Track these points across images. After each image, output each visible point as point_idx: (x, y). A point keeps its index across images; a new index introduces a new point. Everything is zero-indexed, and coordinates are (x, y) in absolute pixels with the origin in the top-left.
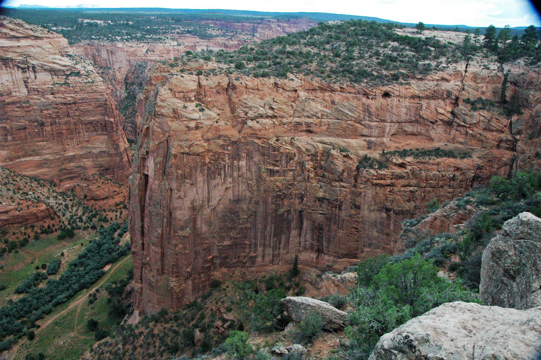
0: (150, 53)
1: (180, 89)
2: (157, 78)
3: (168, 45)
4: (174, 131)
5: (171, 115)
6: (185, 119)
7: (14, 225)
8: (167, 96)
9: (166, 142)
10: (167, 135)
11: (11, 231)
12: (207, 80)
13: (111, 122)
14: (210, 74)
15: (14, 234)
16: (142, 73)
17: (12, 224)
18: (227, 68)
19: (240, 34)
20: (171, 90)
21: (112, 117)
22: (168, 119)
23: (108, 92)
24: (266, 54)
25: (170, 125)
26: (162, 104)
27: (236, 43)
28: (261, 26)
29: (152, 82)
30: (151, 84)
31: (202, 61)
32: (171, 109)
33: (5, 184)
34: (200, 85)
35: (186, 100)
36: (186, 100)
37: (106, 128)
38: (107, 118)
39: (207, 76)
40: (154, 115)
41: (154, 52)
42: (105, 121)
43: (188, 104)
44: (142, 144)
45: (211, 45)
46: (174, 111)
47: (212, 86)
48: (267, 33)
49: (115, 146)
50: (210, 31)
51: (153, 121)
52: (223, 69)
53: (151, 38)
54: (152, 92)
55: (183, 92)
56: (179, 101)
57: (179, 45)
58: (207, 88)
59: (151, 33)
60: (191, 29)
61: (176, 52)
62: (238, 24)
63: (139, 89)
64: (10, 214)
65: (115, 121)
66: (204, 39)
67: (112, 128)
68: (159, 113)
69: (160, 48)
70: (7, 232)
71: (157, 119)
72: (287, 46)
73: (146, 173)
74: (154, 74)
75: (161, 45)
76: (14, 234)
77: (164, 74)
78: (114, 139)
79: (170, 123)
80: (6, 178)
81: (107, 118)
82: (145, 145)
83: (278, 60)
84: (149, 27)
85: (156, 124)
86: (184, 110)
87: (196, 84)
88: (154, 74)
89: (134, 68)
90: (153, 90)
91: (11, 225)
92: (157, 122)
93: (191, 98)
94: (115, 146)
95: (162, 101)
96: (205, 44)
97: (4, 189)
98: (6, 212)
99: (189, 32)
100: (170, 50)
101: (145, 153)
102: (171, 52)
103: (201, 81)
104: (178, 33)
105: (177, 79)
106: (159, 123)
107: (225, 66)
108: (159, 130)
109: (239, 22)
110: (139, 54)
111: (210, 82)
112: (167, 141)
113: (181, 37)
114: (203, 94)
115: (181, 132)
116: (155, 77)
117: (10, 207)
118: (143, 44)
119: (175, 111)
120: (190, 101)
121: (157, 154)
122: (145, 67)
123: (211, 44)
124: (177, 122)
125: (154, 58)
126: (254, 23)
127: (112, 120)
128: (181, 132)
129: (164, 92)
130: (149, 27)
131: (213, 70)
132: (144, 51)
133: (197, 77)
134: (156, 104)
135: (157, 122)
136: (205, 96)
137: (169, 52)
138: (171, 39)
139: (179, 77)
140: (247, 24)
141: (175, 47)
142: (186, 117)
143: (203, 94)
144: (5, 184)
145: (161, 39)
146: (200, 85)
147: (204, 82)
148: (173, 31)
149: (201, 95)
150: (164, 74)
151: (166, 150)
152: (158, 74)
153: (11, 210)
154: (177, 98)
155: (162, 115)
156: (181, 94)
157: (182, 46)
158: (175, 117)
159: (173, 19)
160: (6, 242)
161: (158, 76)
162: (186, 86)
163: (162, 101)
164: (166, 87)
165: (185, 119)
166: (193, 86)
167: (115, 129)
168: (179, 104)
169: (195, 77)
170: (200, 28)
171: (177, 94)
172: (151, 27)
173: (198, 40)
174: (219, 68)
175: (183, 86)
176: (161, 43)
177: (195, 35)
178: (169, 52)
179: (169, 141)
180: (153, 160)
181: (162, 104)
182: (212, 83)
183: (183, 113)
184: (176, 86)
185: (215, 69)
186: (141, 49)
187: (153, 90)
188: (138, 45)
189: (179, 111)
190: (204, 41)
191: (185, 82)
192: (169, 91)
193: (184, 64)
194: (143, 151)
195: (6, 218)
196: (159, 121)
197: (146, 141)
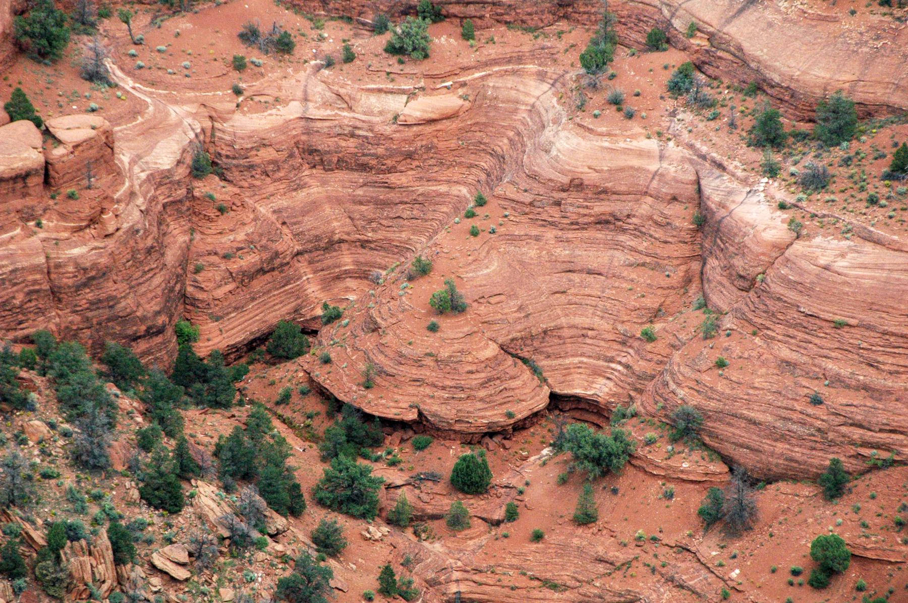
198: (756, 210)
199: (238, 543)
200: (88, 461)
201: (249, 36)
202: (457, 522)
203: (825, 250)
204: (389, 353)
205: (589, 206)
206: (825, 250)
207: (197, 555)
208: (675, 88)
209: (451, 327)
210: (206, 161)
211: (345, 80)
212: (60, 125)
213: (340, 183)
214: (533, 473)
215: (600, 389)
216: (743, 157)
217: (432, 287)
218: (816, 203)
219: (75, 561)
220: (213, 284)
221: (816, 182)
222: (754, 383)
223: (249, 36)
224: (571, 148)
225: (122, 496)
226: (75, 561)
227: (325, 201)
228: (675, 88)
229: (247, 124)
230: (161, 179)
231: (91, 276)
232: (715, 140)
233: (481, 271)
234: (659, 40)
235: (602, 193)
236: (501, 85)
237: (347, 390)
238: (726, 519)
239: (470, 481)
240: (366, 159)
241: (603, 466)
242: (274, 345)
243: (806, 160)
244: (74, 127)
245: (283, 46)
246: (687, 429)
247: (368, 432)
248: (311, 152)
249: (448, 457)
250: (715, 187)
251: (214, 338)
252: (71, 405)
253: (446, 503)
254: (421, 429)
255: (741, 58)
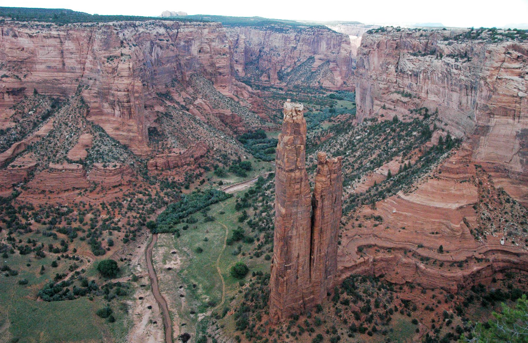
7: (521, 272)
11: (517, 278)
15: (520, 281)
17: (520, 270)
33: (522, 224)
64: (522, 257)
70: (513, 277)
76: (520, 281)
80: (523, 216)
91: (518, 271)
97: (520, 228)
98: (518, 255)
117: (523, 251)
144: (522, 224)
153: (523, 254)
160: (510, 287)
195: (516, 261)
198: (422, 266)
199: (386, 294)
200: (373, 286)
201: (376, 250)
202: (400, 292)
203: (429, 270)
204: (391, 277)
205: (406, 265)
206: (429, 270)
207: (383, 295)
208: (413, 255)
209: (398, 275)
210: (374, 261)
211: (384, 254)
212: (365, 258)
213: (384, 263)
214: (406, 288)
215: (410, 281)
216: (420, 262)
217: (395, 272)
218: (427, 266)
219: (374, 295)
220: (376, 271)
221: (427, 264)
222: (424, 281)
223: (376, 250)
224: (404, 260)
225: (376, 289)
226: (374, 295)
227: (383, 264)
228: (413, 255)
229: (377, 257)
230: (371, 262)
231: (368, 270)
232: (417, 260)
233: (399, 271)
234: (410, 251)
235: (408, 264)
236: (397, 255)
237: (389, 281)
238: (424, 292)
239: (401, 289)
240: (387, 261)
241: (412, 288)
242: (381, 276)
243: (425, 262)
244: (366, 258)
245: (379, 251)
246: (419, 285)
247: (391, 284)
248: (382, 260)
249: (398, 286)
250: (418, 264)
251: (377, 276)
252: (371, 282)
253: (399, 290)
254: (396, 284)
255: (418, 253)
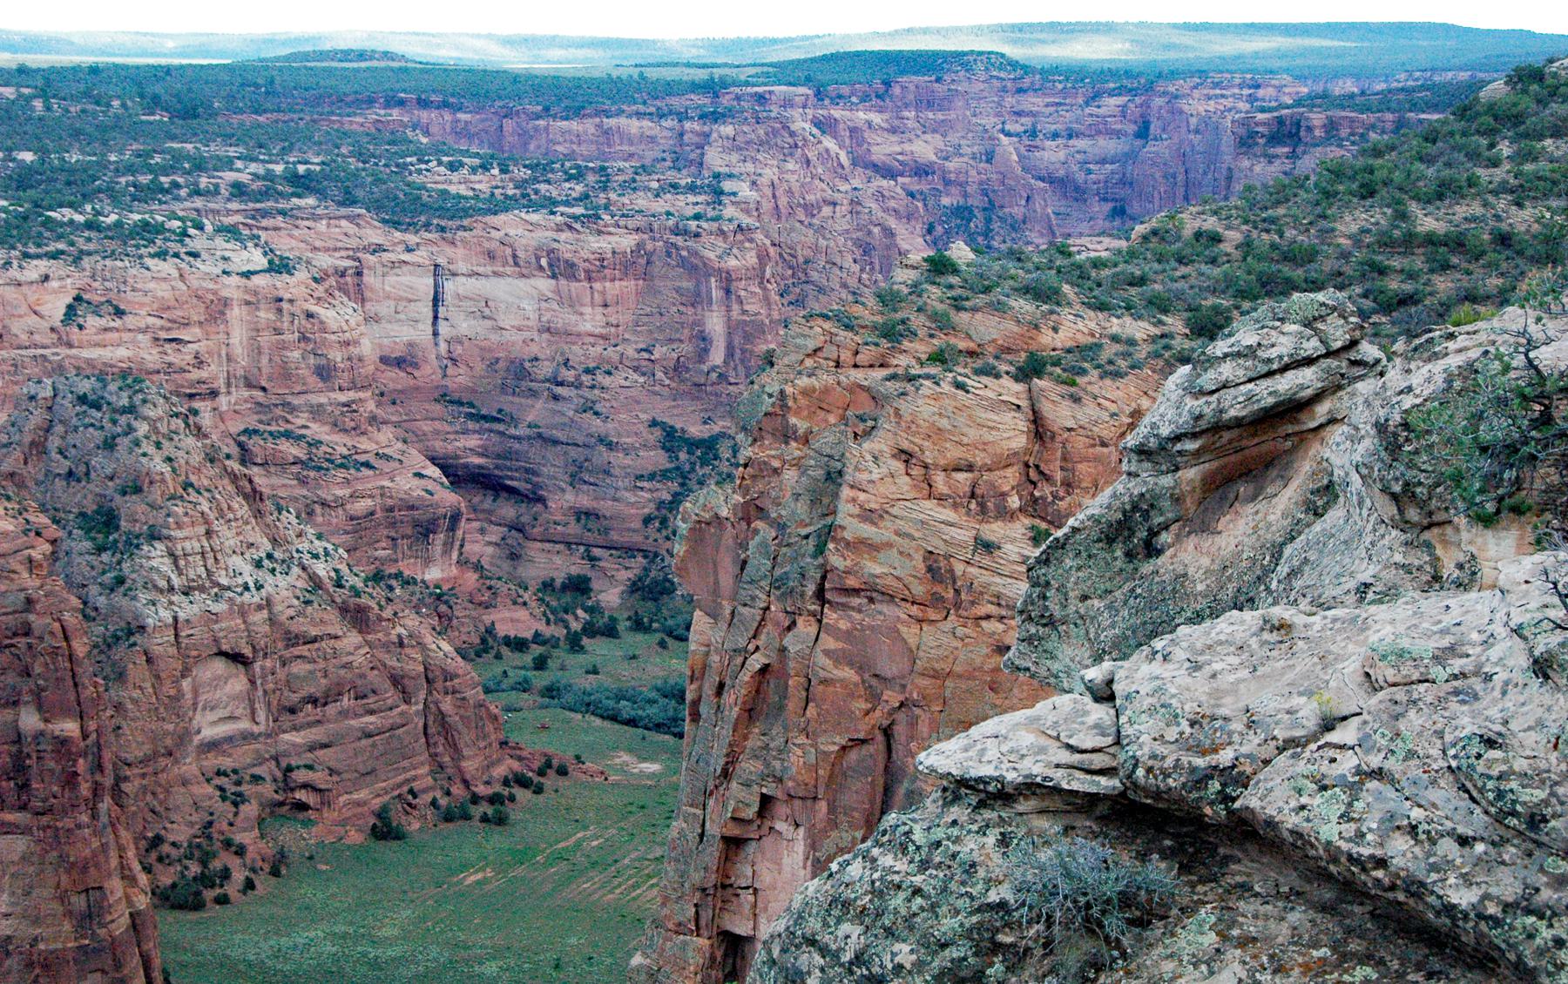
0: (92, 322)
1: (954, 453)
2: (818, 401)
3: (207, 267)
4: (935, 675)
5: (919, 590)
6: (992, 609)
8: (887, 489)
9: (880, 737)
10: (892, 697)
12: (1076, 400)
13: (62, 742)
14: (1083, 372)
16: (109, 445)
18: (1153, 339)
19: (630, 186)
20: (906, 456)
21: (66, 713)
22: (899, 612)
23: (36, 554)
24: (1310, 256)
25: (912, 642)
26: (867, 530)
27: (627, 242)
28: (728, 130)
29: (793, 420)
30: (786, 435)
31: (1024, 306)
32: (918, 557)
34: (1039, 429)
35: (983, 507)
36: (983, 507)
37: (24, 787)
38: (30, 720)
39: (1073, 384)
40: (820, 594)
41: (119, 313)
42: (18, 739)
43: (994, 530)
44: (732, 759)
45: (462, 267)
46: (930, 569)
47: (1105, 434)
48: (769, 174)
49: (79, 902)
50: (436, 178)
51: (806, 628)
52: (1131, 342)
53: (90, 225)
54: (790, 475)
55: (970, 468)
56: (948, 514)
57: (280, 266)
58: (1079, 443)
59: (86, 197)
60: (314, 163)
61: (266, 315)
62: (574, 125)
63: (100, 549)
65: (85, 736)
66: (411, 227)
67: (71, 780)
68: (852, 582)
69: (162, 291)
71: (831, 616)
72: (1414, 207)
73: (742, 928)
74: (804, 381)
75: (167, 267)
77: (857, 375)
78: (79, 852)
79: (910, 633)
81: (30, 720)
82: (749, 767)
83: (1394, 285)
84: (28, 157)
85: (828, 642)
86: (986, 561)
87: (1023, 425)
88: (804, 381)
89: (38, 417)
90: (797, 464)
92: (835, 633)
93: (1004, 495)
94: (79, 902)
95: (868, 515)
96: (421, 256)
99: (302, 184)
100: (226, 302)
101: (750, 812)
102: (236, 313)
103: (1046, 409)
104: (239, 190)
105: (936, 397)
106: (848, 636)
107: (1138, 329)
108: (848, 674)
109: (577, 112)
110: (17, 328)
111: (1088, 412)
112: (887, 732)
113: (265, 214)
114: (1058, 476)
115: (971, 677)
116: (806, 392)
118: (42, 265)
119: (936, 569)
120: (1005, 514)
121: (832, 809)
122: (131, 410)
123: (459, 257)
124: (947, 626)
125: (122, 352)
126: (682, 116)
127: (70, 727)
128: (969, 676)
129: (873, 469)
130: (28, 157)
131: (1090, 348)
132: (56, 307)
133: (1019, 387)
134: (828, 533)
135: (835, 633)
136: (1068, 485)
137: (217, 310)
138: (218, 230)
139: (946, 387)
140: (634, 126)
141: (257, 280)
142: (997, 600)
143: (1058, 476)
145: (160, 229)
146: (1039, 429)
147: (1060, 414)
148: (204, 182)
149: (1048, 478)
150: (857, 375)
151: (881, 781)
152: (825, 379)
154: (941, 499)
155: (871, 592)
156: (961, 476)
157: (301, 275)
158: (936, 600)
159: (155, 103)
161: (826, 390)
162: (988, 437)
163: (868, 515)
164: (880, 443)
165: (992, 609)
166: (1013, 434)
167: (85, 789)
168: (955, 529)
169: (1012, 390)
170: (361, 156)
171: (939, 479)
172: (43, 152)
173: (374, 234)
174: (1115, 339)
175: (973, 434)
176: (162, 255)
177: (349, 200)
178: (217, 310)
179: (900, 731)
180: (800, 847)
181: (867, 530)
182: (1105, 416)
183: (984, 577)
184: (936, 434)
185: (1099, 346)
186: (32, 294)
187: (797, 464)
188: (14, 273)
189: (959, 568)
190: (412, 239)
191: (984, 415)
192: (898, 466)
193: (942, 324)
194: (742, 796)
196: (844, 625)
197: (754, 742)
